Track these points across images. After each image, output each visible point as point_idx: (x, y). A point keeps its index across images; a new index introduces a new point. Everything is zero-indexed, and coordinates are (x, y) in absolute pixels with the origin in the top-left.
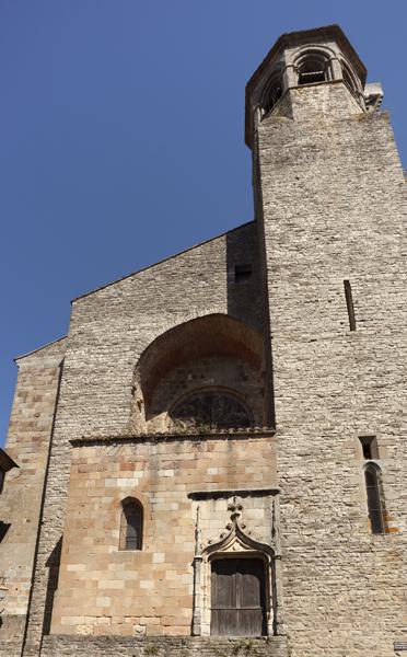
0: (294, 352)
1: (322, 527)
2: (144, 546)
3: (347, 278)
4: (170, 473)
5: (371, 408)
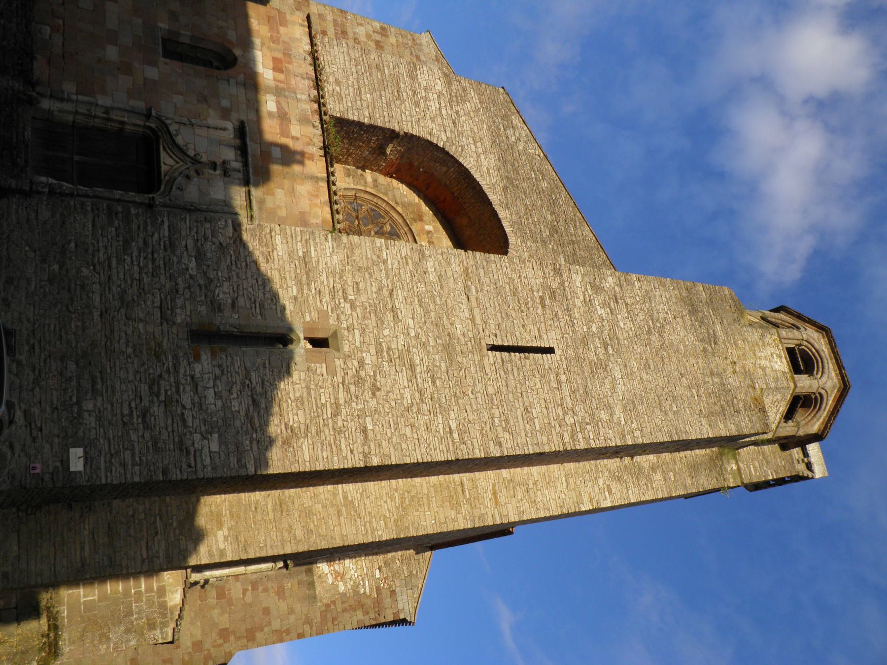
0: (449, 274)
1: (199, 265)
2: (168, 61)
5: (379, 352)
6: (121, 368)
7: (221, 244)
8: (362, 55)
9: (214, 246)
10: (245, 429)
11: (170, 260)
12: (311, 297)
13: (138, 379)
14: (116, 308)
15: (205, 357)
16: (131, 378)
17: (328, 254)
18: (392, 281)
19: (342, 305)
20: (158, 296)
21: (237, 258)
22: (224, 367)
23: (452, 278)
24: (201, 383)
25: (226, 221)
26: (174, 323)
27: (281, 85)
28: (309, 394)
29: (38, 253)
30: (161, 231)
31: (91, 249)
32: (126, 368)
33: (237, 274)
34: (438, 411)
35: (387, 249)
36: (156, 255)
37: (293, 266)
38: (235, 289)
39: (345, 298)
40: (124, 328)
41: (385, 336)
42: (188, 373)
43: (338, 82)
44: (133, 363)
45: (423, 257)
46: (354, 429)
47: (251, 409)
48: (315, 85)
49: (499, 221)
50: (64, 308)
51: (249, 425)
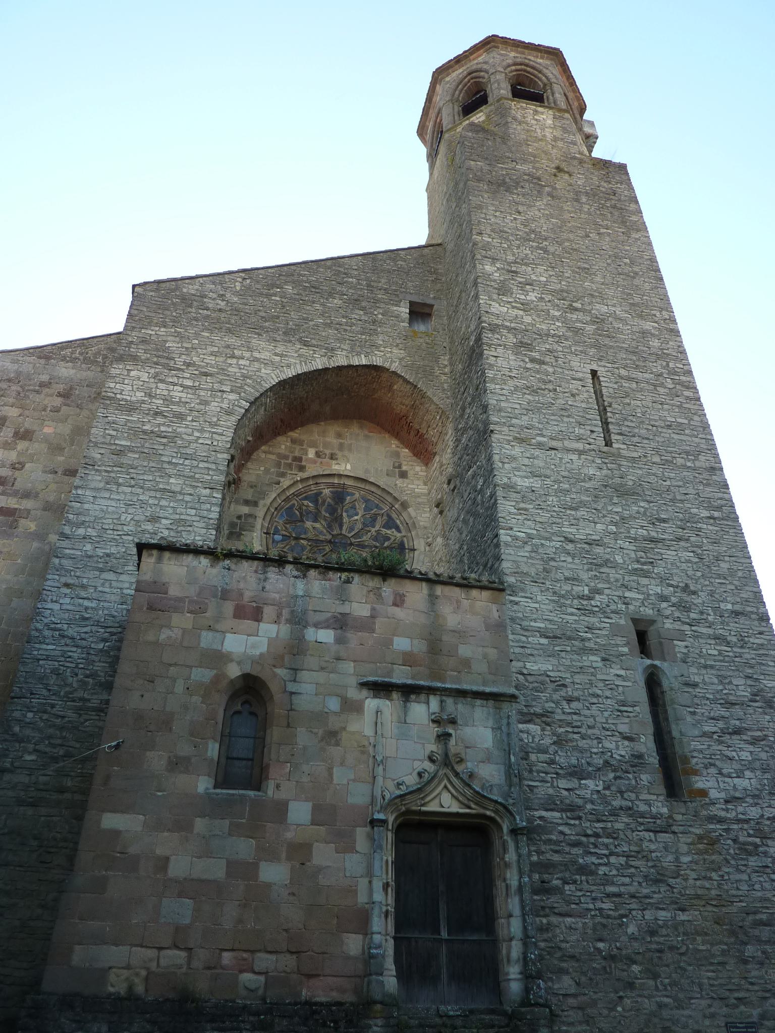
0: (526, 462)
1: (588, 776)
2: (271, 784)
3: (595, 367)
4: (326, 636)
6: (738, 889)
7: (554, 743)
8: (97, 470)
9: (559, 752)
10: (767, 749)
11: (591, 814)
12: (598, 640)
13: (745, 868)
14: (669, 891)
15: (700, 783)
16: (745, 877)
17: (537, 605)
18: (553, 534)
19: (599, 604)
20: (641, 833)
21: (569, 724)
22: (706, 761)
23: (531, 460)
24: (732, 793)
25: (521, 731)
26: (670, 817)
27: (286, 613)
28: (712, 667)
29: (621, 994)
30: (555, 821)
31: (598, 919)
32: (737, 881)
33: (589, 727)
34: (695, 525)
35: (511, 529)
36: (589, 832)
37: (563, 654)
38: (609, 733)
39: (590, 598)
40: (691, 882)
41: (625, 561)
42: (724, 807)
43: (154, 519)
44: (728, 873)
45: (512, 487)
46: (737, 625)
47: (745, 737)
48: (276, 565)
49: (350, 367)
50: (684, 958)
51: (762, 743)
